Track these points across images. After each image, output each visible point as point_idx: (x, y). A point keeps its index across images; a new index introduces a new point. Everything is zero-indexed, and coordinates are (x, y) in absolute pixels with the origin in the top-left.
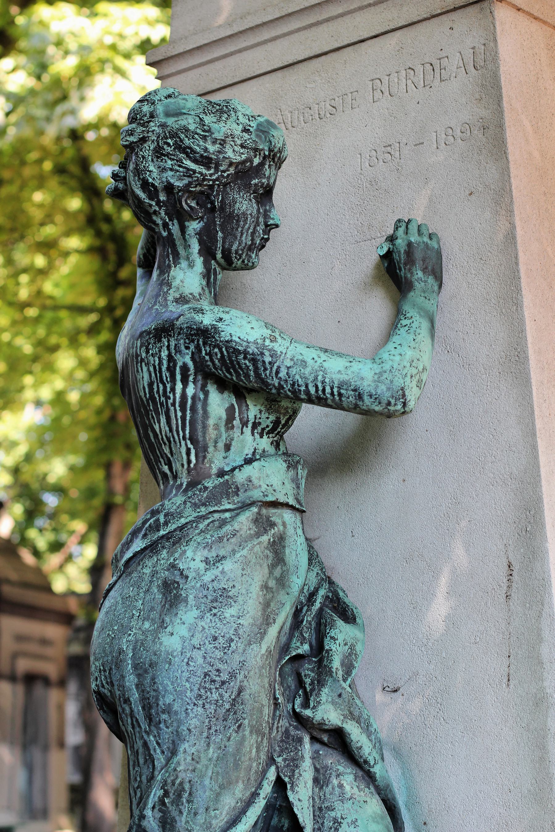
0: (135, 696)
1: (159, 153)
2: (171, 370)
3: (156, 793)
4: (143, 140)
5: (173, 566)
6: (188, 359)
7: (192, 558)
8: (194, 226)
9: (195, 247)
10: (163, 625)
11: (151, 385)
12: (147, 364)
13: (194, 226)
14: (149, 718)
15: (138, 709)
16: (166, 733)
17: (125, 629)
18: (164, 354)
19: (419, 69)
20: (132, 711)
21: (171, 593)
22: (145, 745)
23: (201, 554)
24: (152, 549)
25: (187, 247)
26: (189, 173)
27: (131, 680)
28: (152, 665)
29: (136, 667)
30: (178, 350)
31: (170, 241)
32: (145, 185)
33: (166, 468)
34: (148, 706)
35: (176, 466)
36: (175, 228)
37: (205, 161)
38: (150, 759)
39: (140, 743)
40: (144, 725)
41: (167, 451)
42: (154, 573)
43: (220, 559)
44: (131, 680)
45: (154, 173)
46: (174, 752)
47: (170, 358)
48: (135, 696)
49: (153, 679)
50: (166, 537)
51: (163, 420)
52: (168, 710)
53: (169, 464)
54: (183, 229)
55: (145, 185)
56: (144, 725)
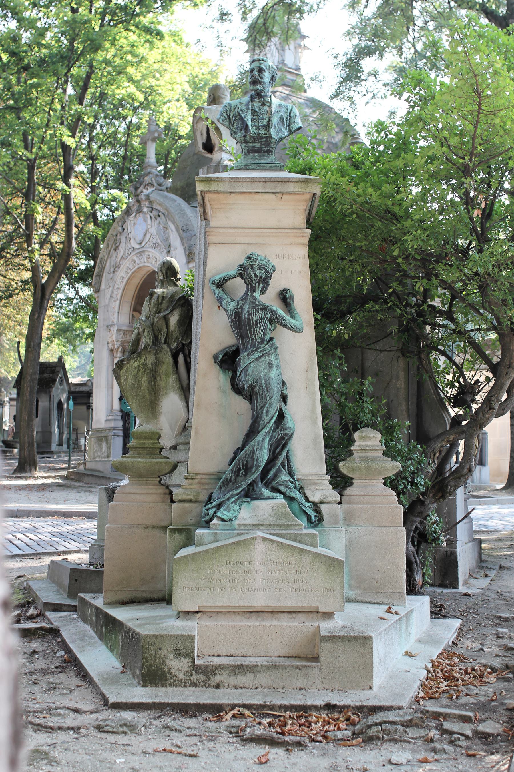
0: (264, 386)
1: (259, 268)
8: (261, 285)
13: (261, 285)
16: (271, 394)
17: (261, 372)
24: (263, 355)
27: (263, 382)
31: (255, 287)
32: (255, 275)
34: (268, 388)
37: (268, 272)
44: (263, 382)
48: (264, 386)
55: (255, 275)
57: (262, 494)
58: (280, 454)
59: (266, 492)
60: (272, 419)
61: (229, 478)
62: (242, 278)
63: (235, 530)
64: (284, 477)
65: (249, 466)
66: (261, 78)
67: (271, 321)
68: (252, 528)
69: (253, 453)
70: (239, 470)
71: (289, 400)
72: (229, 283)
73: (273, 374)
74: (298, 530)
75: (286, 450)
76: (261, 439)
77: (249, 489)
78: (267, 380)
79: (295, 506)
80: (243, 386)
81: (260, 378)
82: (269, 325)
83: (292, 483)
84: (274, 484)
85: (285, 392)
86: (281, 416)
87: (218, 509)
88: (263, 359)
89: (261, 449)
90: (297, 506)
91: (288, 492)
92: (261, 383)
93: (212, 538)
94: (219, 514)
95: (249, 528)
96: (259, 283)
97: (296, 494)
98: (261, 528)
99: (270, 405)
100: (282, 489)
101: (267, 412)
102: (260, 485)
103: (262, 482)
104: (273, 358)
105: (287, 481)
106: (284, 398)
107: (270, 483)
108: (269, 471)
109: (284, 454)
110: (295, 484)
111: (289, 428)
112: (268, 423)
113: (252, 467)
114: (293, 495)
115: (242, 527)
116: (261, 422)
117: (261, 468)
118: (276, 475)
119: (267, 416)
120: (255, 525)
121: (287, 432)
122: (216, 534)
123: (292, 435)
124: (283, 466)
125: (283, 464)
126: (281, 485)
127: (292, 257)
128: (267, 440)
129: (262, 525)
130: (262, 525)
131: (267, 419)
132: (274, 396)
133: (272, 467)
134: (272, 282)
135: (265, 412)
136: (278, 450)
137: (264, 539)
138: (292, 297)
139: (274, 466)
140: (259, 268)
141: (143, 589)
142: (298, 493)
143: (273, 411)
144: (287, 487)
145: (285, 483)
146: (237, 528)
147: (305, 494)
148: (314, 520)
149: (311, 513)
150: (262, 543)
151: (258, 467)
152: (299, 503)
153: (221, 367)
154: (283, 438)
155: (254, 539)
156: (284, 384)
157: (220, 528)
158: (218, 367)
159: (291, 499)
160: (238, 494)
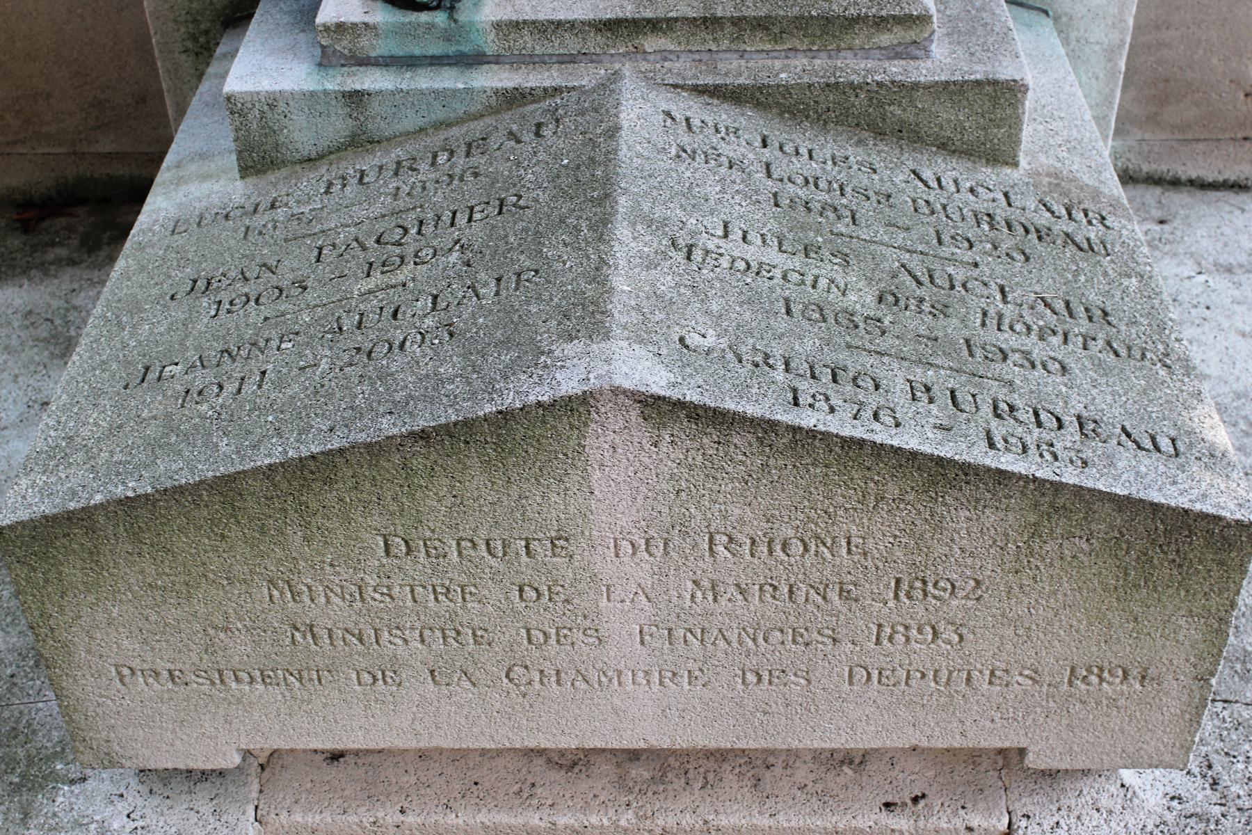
63: (474, 60)
68: (594, 43)
74: (896, 53)
93: (337, 126)
95: (572, 44)
98: (651, 43)
115: (527, 41)
120: (611, 27)
122: (355, 98)
129: (654, 25)
130: (654, 25)
137: (656, 408)
141: (106, 145)
146: (490, 44)
150: (642, 434)
155: (577, 408)
157: (381, 48)
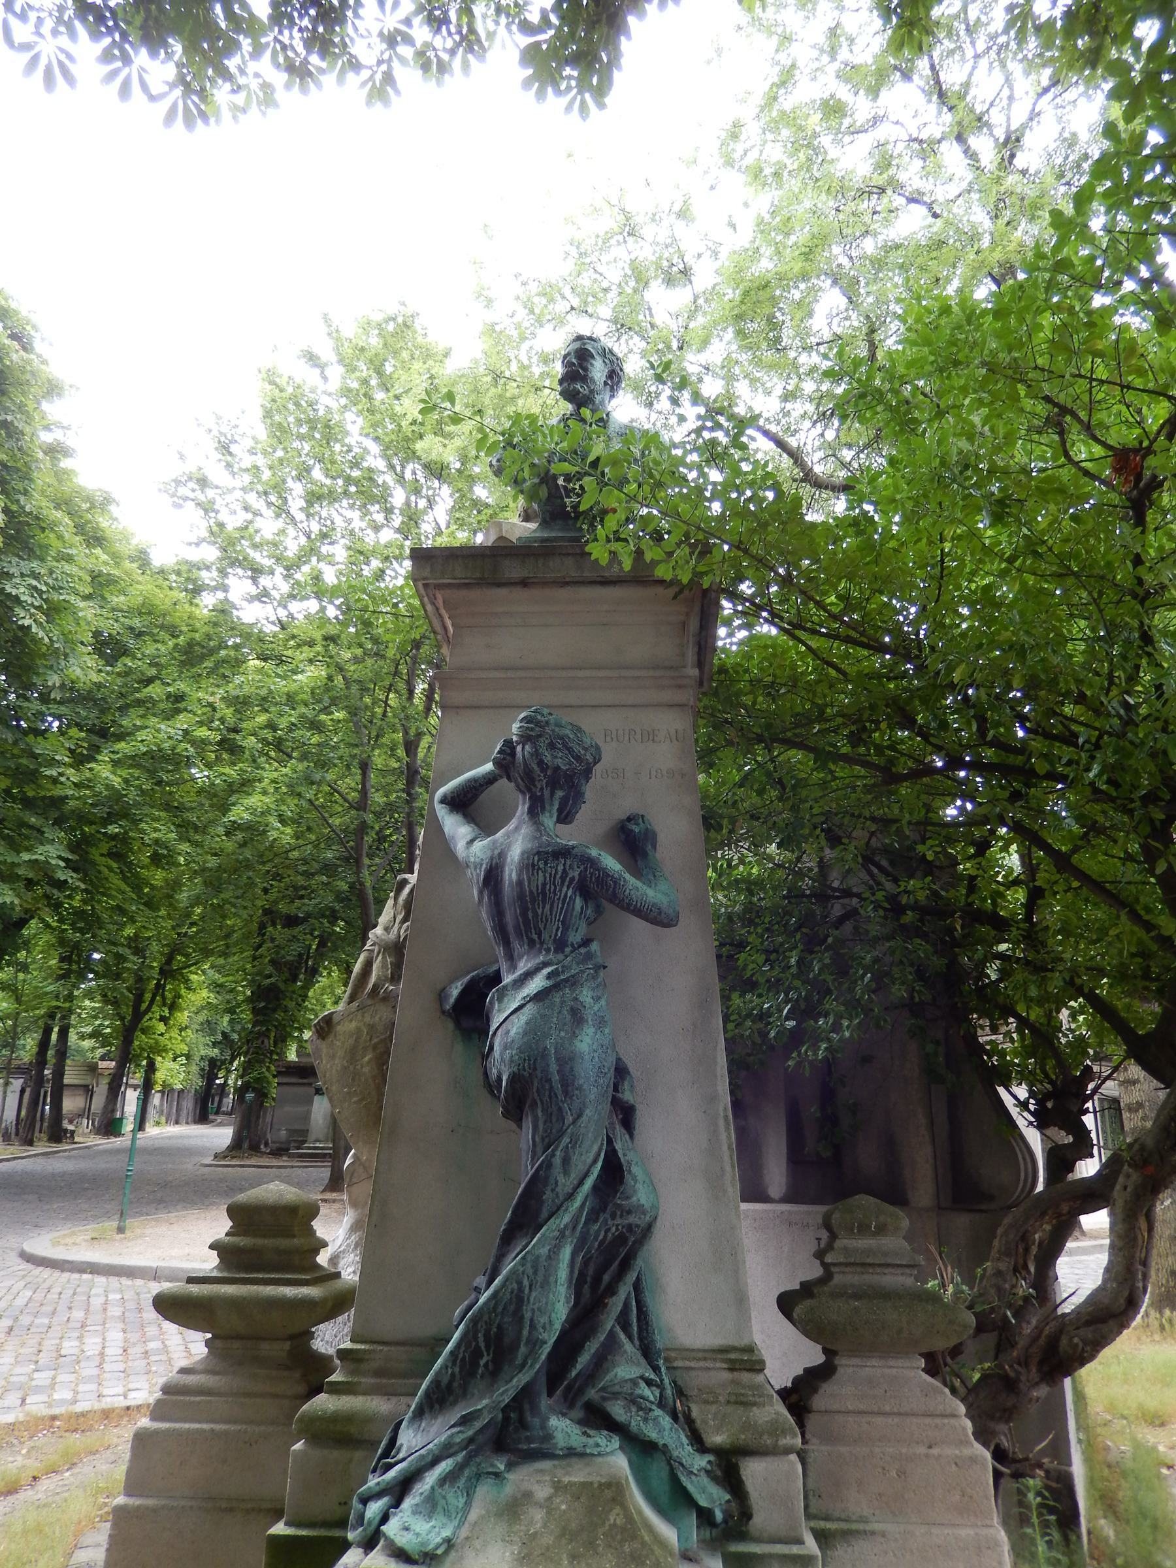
0: (556, 1078)
2: (563, 879)
3: (566, 1140)
4: (540, 736)
5: (576, 999)
6: (576, 874)
7: (586, 995)
8: (560, 794)
9: (556, 807)
10: (574, 1035)
11: (544, 885)
12: (544, 872)
13: (560, 794)
14: (566, 1093)
15: (558, 1086)
18: (560, 868)
19: (639, 732)
20: (551, 1087)
21: (577, 1017)
22: (560, 1110)
23: (590, 994)
25: (552, 805)
26: (570, 763)
27: (554, 1068)
28: (571, 1059)
29: (557, 1059)
30: (571, 867)
33: (535, 937)
34: (568, 1084)
35: (545, 936)
36: (547, 792)
37: (578, 758)
38: (562, 1119)
39: (554, 1108)
40: (561, 1096)
41: (541, 926)
42: (563, 1002)
43: (599, 998)
44: (554, 1068)
45: (547, 757)
46: (580, 1116)
47: (564, 870)
48: (556, 1078)
49: (572, 1069)
50: (566, 980)
51: (548, 907)
52: (580, 1088)
53: (540, 935)
54: (552, 794)
56: (561, 1096)
57: (548, 1437)
58: (611, 1290)
59: (563, 1429)
60: (581, 1183)
61: (445, 1381)
62: (509, 779)
64: (627, 1368)
65: (507, 1341)
66: (586, 370)
67: (583, 889)
69: (519, 1299)
70: (477, 1354)
71: (642, 1119)
72: (484, 797)
73: (586, 1042)
75: (631, 1277)
76: (544, 1251)
77: (506, 1419)
78: (567, 1062)
79: (658, 1471)
80: (499, 1079)
81: (544, 1054)
82: (578, 903)
83: (649, 1383)
84: (592, 1394)
85: (627, 1096)
86: (613, 1173)
87: (397, 1504)
88: (557, 998)
89: (545, 1284)
90: (665, 1474)
91: (636, 1423)
92: (546, 1070)
94: (391, 1528)
96: (553, 784)
97: (662, 1429)
99: (574, 1142)
100: (618, 1411)
101: (566, 1161)
102: (544, 1402)
103: (550, 1395)
104: (586, 995)
105: (634, 1382)
106: (626, 1115)
107: (581, 1391)
108: (577, 1349)
109: (625, 1290)
110: (661, 1387)
111: (641, 1209)
112: (570, 1196)
113: (515, 1347)
114: (653, 1435)
116: (548, 1195)
117: (547, 1349)
118: (601, 1361)
119: (566, 1173)
121: (632, 1219)
123: (648, 1229)
124: (625, 1326)
125: (623, 1320)
126: (616, 1396)
127: (650, 736)
128: (566, 1253)
131: (565, 1183)
132: (588, 1112)
133: (587, 1337)
134: (590, 790)
135: (557, 1161)
136: (606, 1278)
138: (650, 836)
139: (592, 1332)
140: (552, 746)
142: (666, 1421)
143: (588, 1157)
144: (634, 1401)
145: (627, 1388)
147: (690, 1422)
148: (719, 1516)
149: (710, 1495)
151: (535, 1344)
152: (669, 1460)
153: (458, 1024)
154: (621, 1239)
156: (621, 1071)
158: (451, 1025)
159: (643, 1449)
160: (471, 1440)
